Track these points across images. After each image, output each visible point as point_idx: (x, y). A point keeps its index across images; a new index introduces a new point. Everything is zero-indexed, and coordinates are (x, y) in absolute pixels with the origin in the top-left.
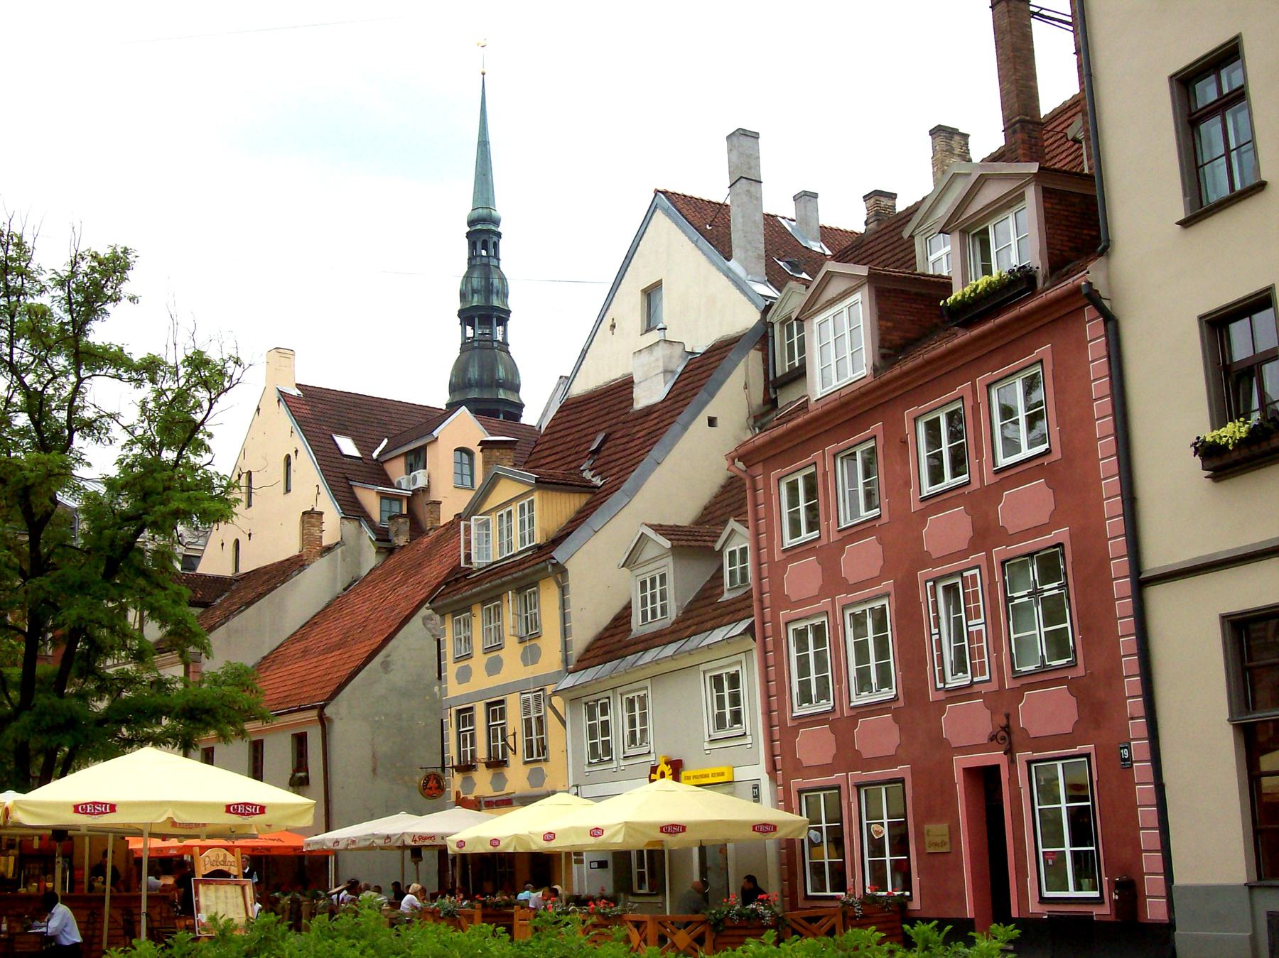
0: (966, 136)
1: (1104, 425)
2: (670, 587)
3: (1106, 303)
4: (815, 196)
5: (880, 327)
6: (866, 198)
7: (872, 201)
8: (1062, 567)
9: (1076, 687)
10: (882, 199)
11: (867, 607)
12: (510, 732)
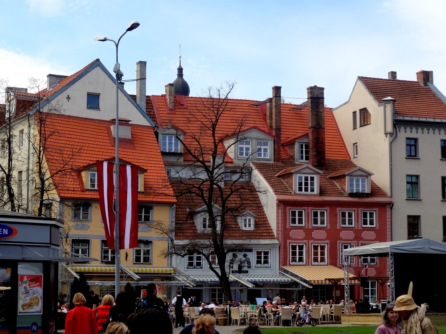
9: (376, 269)
11: (319, 245)
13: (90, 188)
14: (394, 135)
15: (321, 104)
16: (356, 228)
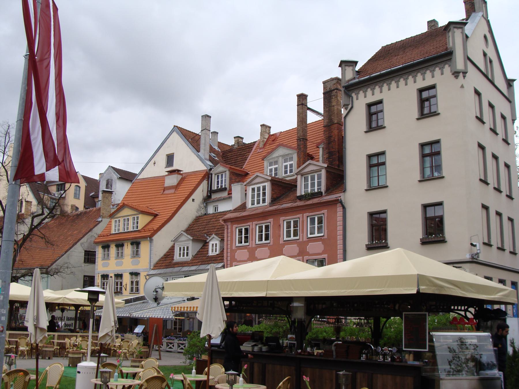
0: (270, 127)
1: (340, 232)
2: (190, 249)
3: (344, 204)
4: (217, 133)
5: (272, 193)
6: (235, 138)
7: (237, 139)
8: (324, 264)
10: (239, 139)
12: (124, 284)
13: (114, 233)
14: (350, 107)
15: (334, 97)
16: (301, 240)
